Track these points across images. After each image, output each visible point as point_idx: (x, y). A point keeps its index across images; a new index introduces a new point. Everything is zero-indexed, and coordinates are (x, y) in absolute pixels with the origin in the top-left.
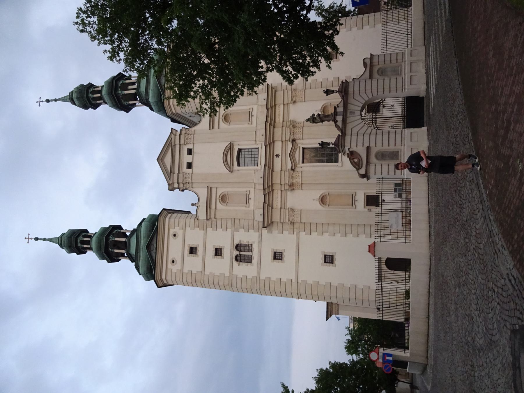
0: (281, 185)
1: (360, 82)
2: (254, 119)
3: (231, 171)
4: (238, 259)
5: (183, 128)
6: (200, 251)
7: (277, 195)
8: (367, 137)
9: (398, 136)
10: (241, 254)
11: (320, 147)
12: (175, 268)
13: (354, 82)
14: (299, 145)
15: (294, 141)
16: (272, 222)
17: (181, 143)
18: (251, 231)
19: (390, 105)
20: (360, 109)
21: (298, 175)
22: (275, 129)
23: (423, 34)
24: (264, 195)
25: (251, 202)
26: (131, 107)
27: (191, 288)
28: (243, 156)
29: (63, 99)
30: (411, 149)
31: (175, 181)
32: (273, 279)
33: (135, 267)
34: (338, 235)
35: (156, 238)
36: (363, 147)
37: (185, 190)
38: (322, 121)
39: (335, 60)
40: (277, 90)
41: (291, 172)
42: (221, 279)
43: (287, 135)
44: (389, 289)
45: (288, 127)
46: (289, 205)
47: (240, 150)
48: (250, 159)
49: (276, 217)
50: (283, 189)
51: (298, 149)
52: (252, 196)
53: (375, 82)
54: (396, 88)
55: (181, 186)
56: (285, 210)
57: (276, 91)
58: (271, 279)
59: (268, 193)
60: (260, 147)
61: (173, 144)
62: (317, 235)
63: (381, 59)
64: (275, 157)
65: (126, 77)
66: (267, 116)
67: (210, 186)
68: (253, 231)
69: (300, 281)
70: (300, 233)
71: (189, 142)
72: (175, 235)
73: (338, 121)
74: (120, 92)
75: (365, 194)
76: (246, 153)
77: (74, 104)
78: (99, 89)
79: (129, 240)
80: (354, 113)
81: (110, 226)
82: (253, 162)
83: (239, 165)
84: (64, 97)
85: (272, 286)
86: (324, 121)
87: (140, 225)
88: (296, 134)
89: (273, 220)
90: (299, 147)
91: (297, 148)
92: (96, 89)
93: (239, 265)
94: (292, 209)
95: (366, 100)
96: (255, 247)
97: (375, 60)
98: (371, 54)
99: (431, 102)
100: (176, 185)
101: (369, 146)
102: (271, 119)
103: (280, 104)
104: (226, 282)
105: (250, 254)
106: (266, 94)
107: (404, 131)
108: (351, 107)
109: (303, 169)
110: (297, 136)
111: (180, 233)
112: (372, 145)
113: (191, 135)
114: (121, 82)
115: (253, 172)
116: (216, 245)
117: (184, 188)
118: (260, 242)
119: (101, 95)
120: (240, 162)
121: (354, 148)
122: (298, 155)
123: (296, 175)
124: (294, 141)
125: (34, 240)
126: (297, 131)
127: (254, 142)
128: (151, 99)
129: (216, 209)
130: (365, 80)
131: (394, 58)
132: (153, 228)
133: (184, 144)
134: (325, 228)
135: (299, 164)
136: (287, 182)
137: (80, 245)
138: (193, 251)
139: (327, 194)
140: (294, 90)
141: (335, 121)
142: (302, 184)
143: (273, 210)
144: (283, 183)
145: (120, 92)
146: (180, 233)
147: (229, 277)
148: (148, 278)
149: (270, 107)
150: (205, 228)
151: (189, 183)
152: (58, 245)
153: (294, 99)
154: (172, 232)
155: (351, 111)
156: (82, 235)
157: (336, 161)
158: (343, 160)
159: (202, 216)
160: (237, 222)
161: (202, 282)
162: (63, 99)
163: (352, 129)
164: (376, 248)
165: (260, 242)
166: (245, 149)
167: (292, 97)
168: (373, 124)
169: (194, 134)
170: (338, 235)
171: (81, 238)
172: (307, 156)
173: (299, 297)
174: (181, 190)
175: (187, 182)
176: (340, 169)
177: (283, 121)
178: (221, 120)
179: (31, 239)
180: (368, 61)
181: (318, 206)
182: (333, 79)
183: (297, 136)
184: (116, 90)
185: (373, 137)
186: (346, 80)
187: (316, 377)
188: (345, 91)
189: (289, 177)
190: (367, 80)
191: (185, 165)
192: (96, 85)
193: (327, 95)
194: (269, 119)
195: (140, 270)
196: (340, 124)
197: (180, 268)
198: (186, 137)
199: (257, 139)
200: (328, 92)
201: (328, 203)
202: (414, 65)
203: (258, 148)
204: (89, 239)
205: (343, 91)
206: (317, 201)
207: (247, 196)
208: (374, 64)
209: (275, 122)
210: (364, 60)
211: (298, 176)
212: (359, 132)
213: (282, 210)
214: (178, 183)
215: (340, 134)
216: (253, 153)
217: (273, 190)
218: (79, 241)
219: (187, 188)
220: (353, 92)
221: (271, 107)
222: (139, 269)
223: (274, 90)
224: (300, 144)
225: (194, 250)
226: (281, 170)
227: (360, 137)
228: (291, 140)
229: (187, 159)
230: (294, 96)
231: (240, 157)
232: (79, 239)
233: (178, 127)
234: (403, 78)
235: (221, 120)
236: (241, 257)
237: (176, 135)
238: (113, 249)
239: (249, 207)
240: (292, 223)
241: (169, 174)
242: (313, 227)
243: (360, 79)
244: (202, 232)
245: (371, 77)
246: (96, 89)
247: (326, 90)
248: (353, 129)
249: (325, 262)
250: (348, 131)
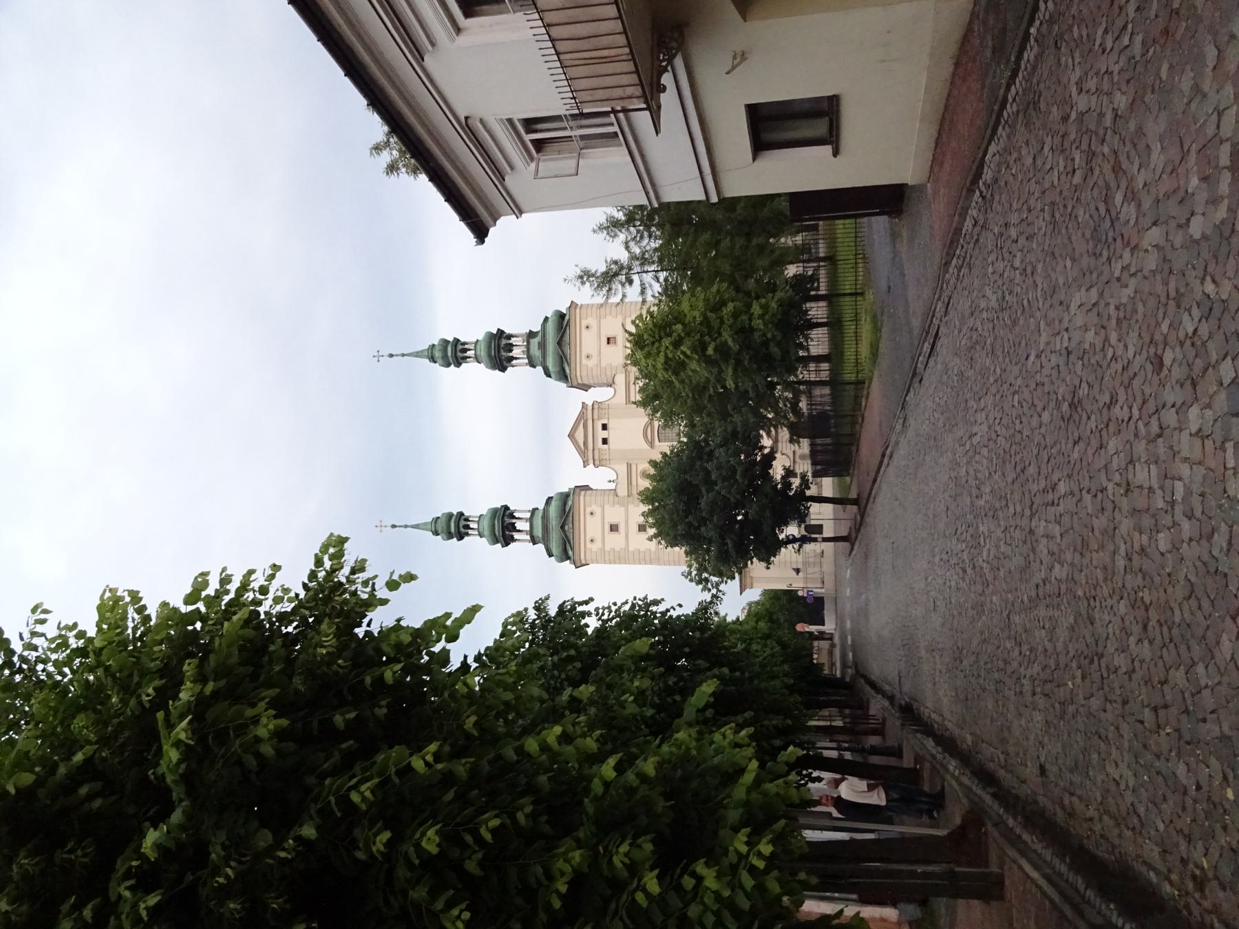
6: (622, 528)
74: (503, 354)
104: (653, 556)
111: (598, 511)
138: (614, 528)
145: (503, 354)
146: (598, 511)
184: (499, 352)
197: (600, 546)
229: (604, 434)
241: (583, 453)
244: (623, 509)
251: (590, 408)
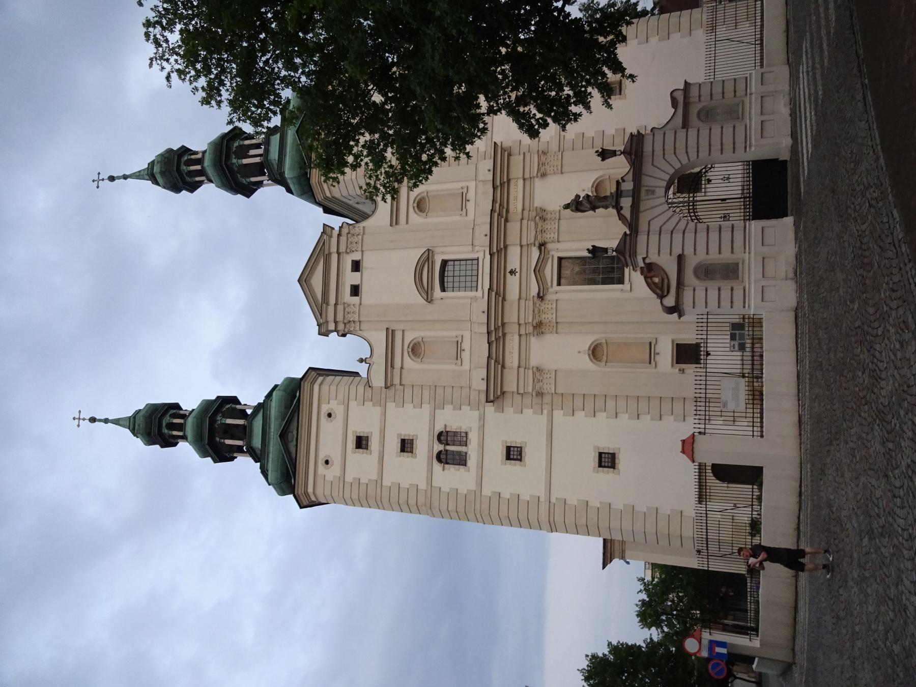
0: (519, 325)
1: (664, 134)
2: (471, 206)
3: (429, 300)
4: (442, 458)
5: (345, 225)
6: (374, 444)
7: (512, 343)
8: (677, 237)
9: (738, 236)
10: (447, 450)
11: (590, 255)
12: (331, 473)
13: (654, 135)
14: (552, 253)
15: (542, 246)
16: (503, 393)
17: (341, 251)
18: (466, 408)
19: (722, 177)
20: (664, 183)
21: (550, 306)
22: (509, 224)
23: (785, 43)
24: (488, 343)
25: (466, 356)
26: (255, 187)
27: (358, 509)
28: (451, 274)
29: (138, 176)
30: (763, 258)
31: (331, 317)
32: (506, 495)
33: (260, 470)
34: (624, 417)
35: (296, 422)
36: (671, 255)
37: (348, 335)
38: (594, 208)
39: (618, 96)
40: (512, 154)
41: (538, 302)
42: (413, 493)
43: (530, 236)
44: (719, 516)
45: (532, 220)
46: (534, 362)
47: (444, 263)
48: (463, 279)
49: (510, 384)
50: (523, 332)
51: (550, 260)
52: (466, 345)
53: (692, 133)
54: (734, 143)
55: (341, 327)
56: (526, 370)
57: (509, 155)
58: (501, 496)
59: (496, 339)
60: (481, 255)
61: (326, 252)
62: (586, 416)
63: (705, 91)
64: (508, 275)
65: (246, 135)
66: (494, 201)
68: (469, 407)
69: (553, 500)
70: (555, 412)
71: (354, 249)
72: (330, 415)
73: (624, 209)
75: (673, 341)
76: (457, 268)
77: (156, 182)
78: (199, 156)
79: (251, 424)
80: (653, 192)
81: (218, 397)
82: (468, 284)
83: (443, 289)
84: (140, 172)
85: (504, 508)
86: (598, 207)
87: (269, 396)
89: (505, 389)
90: (553, 256)
91: (549, 257)
92: (193, 157)
93: (443, 470)
94: (539, 369)
95: (677, 168)
96: (473, 437)
97: (694, 92)
98: (686, 82)
99: (803, 168)
100: (332, 326)
101: (683, 254)
102: (500, 205)
103: (518, 179)
104: (421, 500)
105: (462, 449)
106: (492, 160)
107: (750, 225)
108: (647, 181)
109: (559, 296)
110: (548, 236)
111: (339, 410)
112: (689, 250)
113: (359, 236)
114: (236, 144)
115: (469, 301)
116: (403, 433)
117: (346, 330)
118: (482, 428)
119: (202, 167)
120: (446, 284)
121: (653, 258)
122: (550, 271)
123: (547, 306)
124: (542, 246)
125: (88, 421)
126: (549, 226)
127: (470, 247)
128: (289, 173)
129: (402, 368)
130: (673, 131)
131: (729, 87)
132: (292, 402)
133: (347, 253)
134: (600, 403)
135: (552, 286)
136: (530, 320)
137: (166, 431)
138: (361, 443)
139: (604, 341)
141: (619, 209)
142: (557, 323)
144: (522, 322)
145: (234, 161)
146: (339, 410)
147: (426, 490)
148: (283, 492)
149: (498, 183)
150: (383, 402)
151: (354, 322)
152: (128, 430)
153: (542, 170)
154: (325, 409)
155: (647, 188)
156: (170, 413)
157: (621, 281)
158: (633, 279)
159: (378, 381)
160: (440, 391)
161: (378, 499)
162: (138, 176)
163: (649, 222)
164: (695, 446)
165: (482, 428)
166: (454, 261)
167: (538, 166)
168: (689, 212)
169: (364, 234)
170: (624, 417)
171: (169, 418)
172: (566, 272)
173: (553, 528)
174: (340, 334)
175: (351, 320)
176: (627, 295)
177: (523, 210)
178: (411, 209)
179: (84, 419)
180: (680, 96)
181: (586, 363)
182: (613, 132)
183: (548, 236)
184: (228, 157)
185: (690, 237)
186: (638, 132)
187: (584, 669)
188: (636, 151)
189: (534, 311)
190: (678, 131)
191: (348, 290)
192: (194, 149)
193: (603, 160)
194: (498, 205)
195: (269, 477)
196: (627, 212)
198: (350, 240)
199: (476, 243)
200: (605, 154)
201: (605, 358)
202: (768, 100)
203: (478, 259)
204: (181, 421)
205: (633, 151)
206: (585, 354)
207: (458, 345)
208: (691, 100)
209: (508, 211)
210: (672, 93)
211: (550, 308)
212: (663, 227)
213: (522, 370)
214: (336, 322)
215: (628, 232)
216: (469, 267)
217: (504, 335)
218: (164, 424)
219: (351, 331)
220: (651, 154)
221: (502, 185)
222: (267, 475)
223: (506, 153)
225: (364, 442)
226: (520, 299)
227: (666, 238)
228: (537, 243)
229: (352, 278)
230: (543, 164)
231: (446, 275)
232: (164, 421)
233: (336, 222)
234: (746, 126)
235: (411, 209)
236: (446, 455)
237: (331, 236)
238: (222, 439)
239: (461, 365)
240: (540, 394)
241: (319, 308)
242: (579, 402)
243: (664, 129)
244: (378, 409)
245: (685, 125)
246: (193, 157)
247: (600, 150)
248: (651, 223)
249: (600, 466)
250: (643, 226)
251: (335, 233)
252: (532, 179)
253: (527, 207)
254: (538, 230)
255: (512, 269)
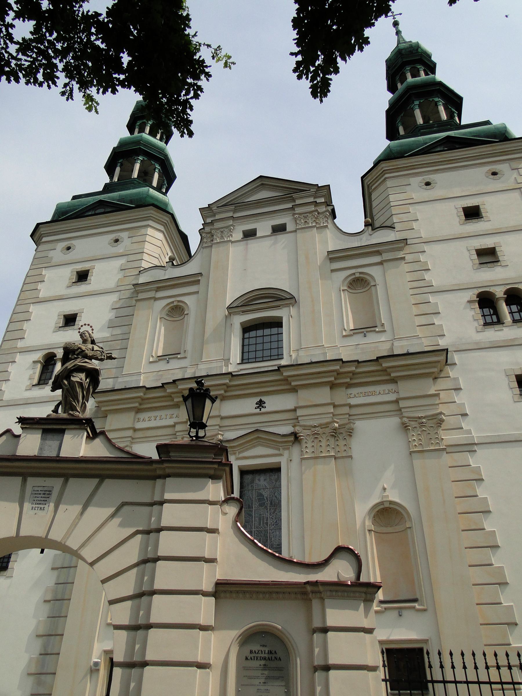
14: (286, 453)
15: (296, 437)
51: (276, 452)
61: (294, 195)
67: (202, 280)
88: (316, 441)
89: (109, 417)
90: (281, 455)
102: (354, 373)
110: (309, 445)
111: (120, 249)
124: (296, 437)
135: (237, 459)
140: (442, 421)
143: (132, 414)
149: (385, 365)
167: (420, 418)
169: (318, 228)
175: (215, 237)
177: (351, 406)
198: (309, 215)
209: (349, 386)
213: (130, 433)
221: (385, 370)
224: (290, 455)
226: (222, 418)
228: (298, 429)
252: (398, 413)
253: (354, 411)
254: (316, 429)
255: (265, 403)
